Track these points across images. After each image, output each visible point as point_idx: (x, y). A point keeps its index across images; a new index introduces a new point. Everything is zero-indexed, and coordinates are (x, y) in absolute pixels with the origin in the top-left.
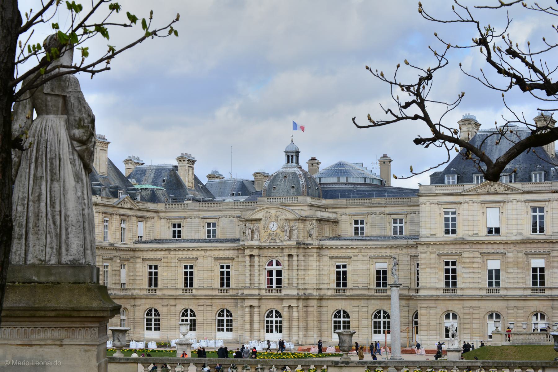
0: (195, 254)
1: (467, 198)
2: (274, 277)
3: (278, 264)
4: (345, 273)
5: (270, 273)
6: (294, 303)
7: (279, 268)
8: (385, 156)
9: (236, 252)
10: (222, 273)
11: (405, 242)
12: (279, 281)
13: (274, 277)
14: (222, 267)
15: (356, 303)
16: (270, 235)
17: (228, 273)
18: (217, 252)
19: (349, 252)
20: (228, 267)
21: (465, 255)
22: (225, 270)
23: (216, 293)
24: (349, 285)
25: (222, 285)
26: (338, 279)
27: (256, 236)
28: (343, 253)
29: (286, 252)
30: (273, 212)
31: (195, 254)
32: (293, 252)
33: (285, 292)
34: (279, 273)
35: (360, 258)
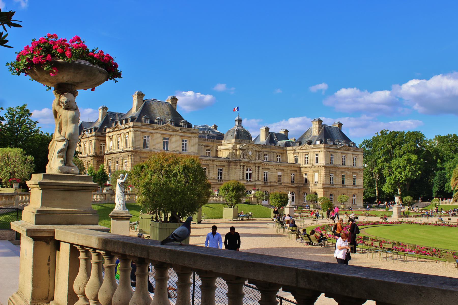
0: (208, 163)
1: (338, 151)
2: (249, 176)
3: (250, 170)
4: (267, 175)
5: (247, 174)
6: (260, 188)
7: (251, 172)
8: (215, 125)
9: (226, 163)
10: (219, 172)
11: (270, 163)
12: (250, 178)
13: (249, 176)
14: (219, 170)
15: (272, 188)
16: (249, 157)
17: (221, 173)
18: (218, 162)
19: (270, 167)
20: (221, 170)
21: (337, 172)
22: (220, 171)
23: (217, 181)
24: (269, 181)
25: (218, 178)
26: (264, 178)
27: (245, 157)
28: (267, 167)
29: (257, 165)
30: (250, 147)
31: (208, 163)
32: (260, 165)
33: (253, 183)
34: (250, 174)
35: (273, 169)
